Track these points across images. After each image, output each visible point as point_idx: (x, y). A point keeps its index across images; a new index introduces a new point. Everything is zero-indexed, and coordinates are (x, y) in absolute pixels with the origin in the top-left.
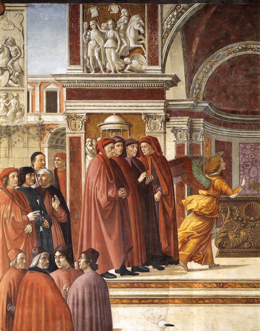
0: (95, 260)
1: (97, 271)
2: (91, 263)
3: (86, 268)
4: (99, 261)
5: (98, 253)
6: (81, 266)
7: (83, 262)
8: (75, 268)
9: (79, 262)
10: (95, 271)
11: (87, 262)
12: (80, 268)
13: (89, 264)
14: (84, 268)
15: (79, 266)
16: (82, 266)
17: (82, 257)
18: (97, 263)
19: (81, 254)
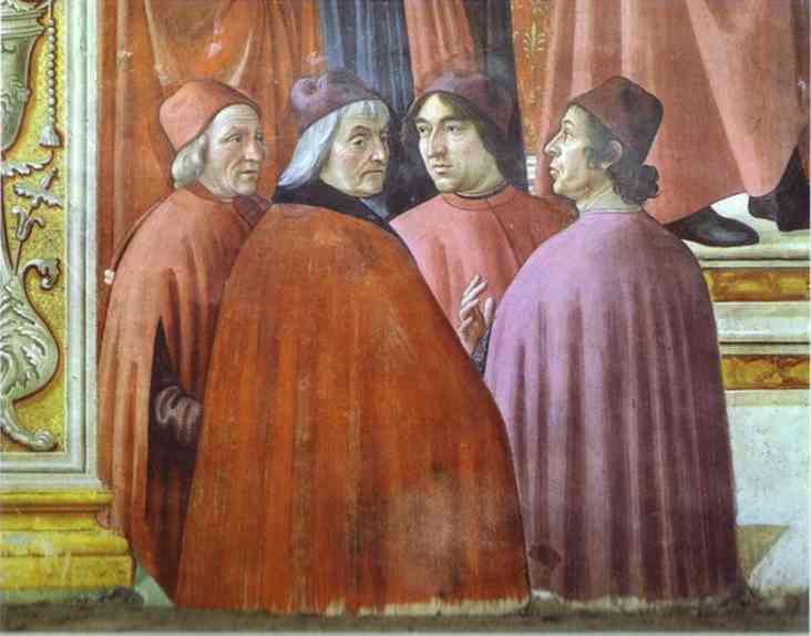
0: (642, 138)
1: (651, 206)
2: (616, 160)
3: (588, 187)
4: (661, 144)
5: (656, 105)
6: (563, 176)
7: (573, 156)
8: (531, 188)
9: (549, 158)
10: (640, 203)
11: (594, 154)
12: (557, 187)
13: (605, 166)
14: (578, 190)
15: (552, 180)
16: (570, 178)
17: (569, 126)
18: (649, 161)
19: (560, 107)
